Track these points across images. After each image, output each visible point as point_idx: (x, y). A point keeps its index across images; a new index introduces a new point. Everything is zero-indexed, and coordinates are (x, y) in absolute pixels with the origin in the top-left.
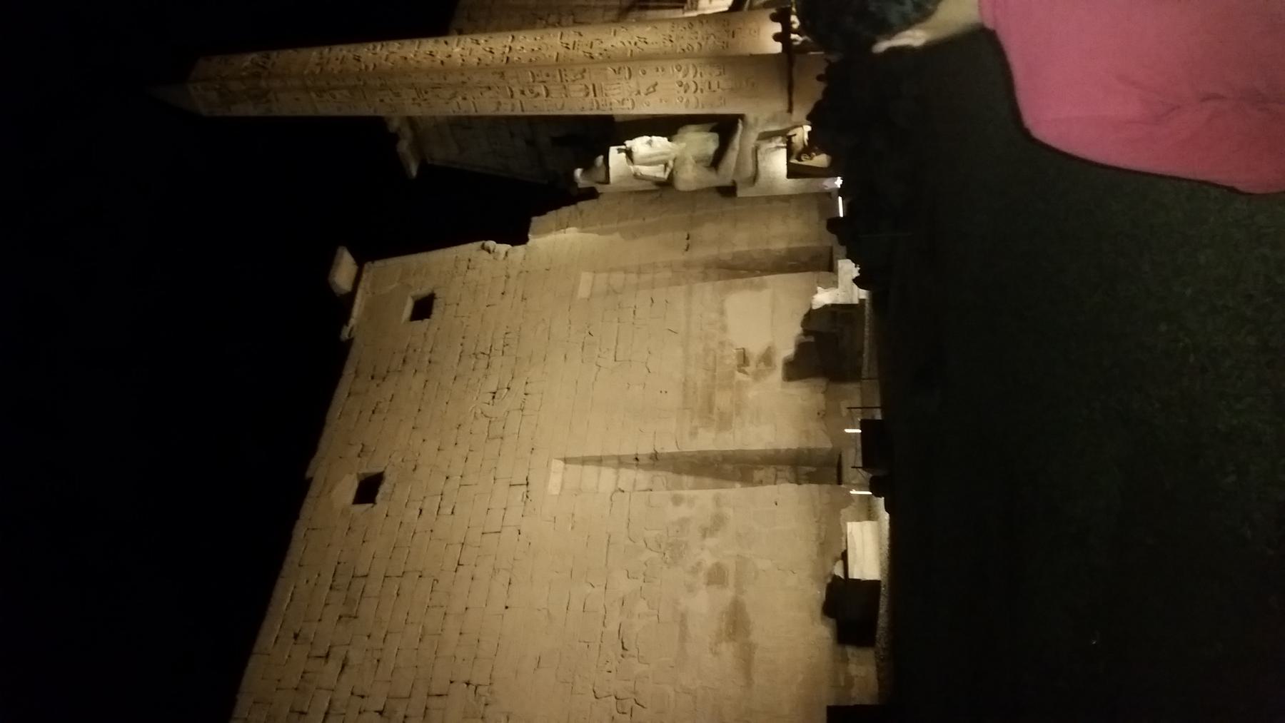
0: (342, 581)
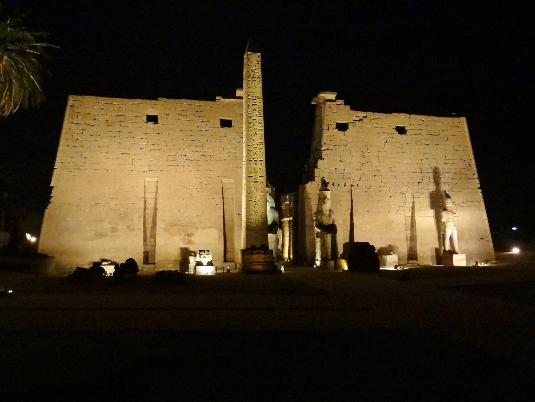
0: (119, 119)
